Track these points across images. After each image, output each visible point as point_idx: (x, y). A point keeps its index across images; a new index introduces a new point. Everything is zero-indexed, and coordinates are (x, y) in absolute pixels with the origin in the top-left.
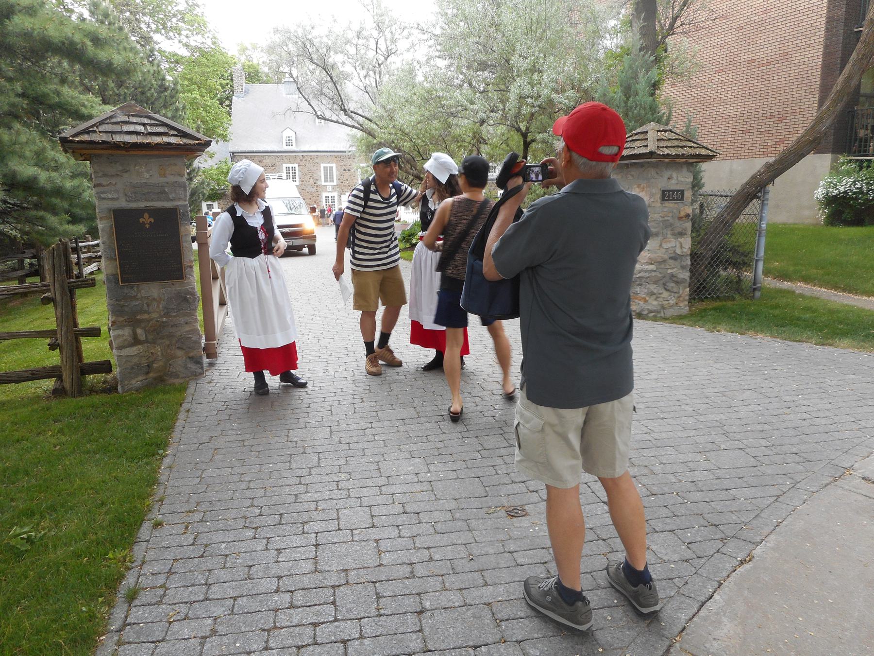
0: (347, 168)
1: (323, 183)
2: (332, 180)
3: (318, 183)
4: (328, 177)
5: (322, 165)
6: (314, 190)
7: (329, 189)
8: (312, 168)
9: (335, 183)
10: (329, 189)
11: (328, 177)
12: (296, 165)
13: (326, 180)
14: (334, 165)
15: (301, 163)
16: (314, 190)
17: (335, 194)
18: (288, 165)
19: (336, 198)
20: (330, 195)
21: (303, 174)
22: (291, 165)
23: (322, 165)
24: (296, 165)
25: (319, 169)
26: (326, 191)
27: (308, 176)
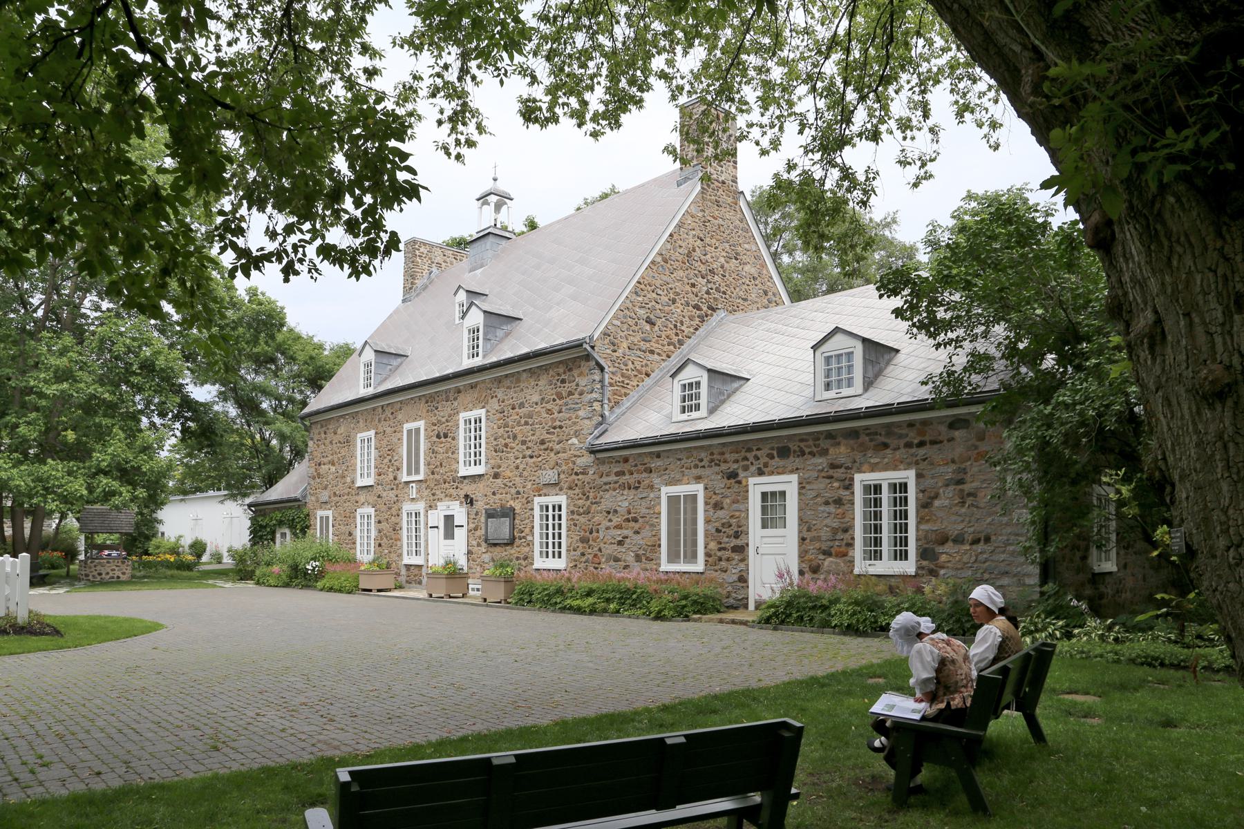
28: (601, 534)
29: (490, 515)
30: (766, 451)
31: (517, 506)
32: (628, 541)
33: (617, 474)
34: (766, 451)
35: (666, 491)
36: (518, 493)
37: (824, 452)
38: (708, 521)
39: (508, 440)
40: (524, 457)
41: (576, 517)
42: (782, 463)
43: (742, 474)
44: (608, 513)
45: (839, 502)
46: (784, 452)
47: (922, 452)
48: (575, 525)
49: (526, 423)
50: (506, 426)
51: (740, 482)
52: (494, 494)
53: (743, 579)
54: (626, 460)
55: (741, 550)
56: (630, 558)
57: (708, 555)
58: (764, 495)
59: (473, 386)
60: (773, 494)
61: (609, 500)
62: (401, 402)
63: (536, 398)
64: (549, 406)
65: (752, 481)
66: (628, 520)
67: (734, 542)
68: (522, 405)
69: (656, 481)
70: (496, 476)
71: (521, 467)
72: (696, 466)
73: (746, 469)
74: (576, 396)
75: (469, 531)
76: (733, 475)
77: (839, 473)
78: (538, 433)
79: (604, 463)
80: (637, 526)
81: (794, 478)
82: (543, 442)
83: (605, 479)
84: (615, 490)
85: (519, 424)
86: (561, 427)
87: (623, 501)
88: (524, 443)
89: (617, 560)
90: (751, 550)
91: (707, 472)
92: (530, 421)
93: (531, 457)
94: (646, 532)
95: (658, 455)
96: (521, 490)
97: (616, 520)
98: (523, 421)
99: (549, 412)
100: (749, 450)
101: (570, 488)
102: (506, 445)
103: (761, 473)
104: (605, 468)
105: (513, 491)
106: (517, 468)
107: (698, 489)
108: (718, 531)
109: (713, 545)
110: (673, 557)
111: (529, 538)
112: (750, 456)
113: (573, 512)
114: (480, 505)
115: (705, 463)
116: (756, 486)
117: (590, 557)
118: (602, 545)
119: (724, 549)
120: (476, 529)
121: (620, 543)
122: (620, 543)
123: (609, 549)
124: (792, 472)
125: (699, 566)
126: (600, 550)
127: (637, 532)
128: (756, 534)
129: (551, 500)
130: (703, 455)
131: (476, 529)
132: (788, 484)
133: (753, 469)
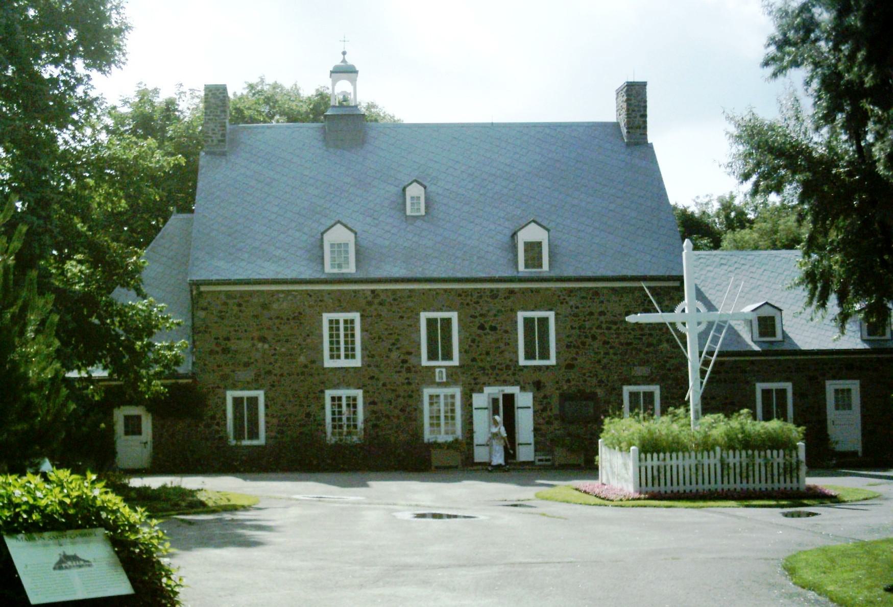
1: (425, 362)
2: (448, 356)
3: (412, 360)
6: (400, 379)
7: (441, 375)
9: (455, 362)
10: (441, 375)
12: (356, 316)
13: (432, 356)
14: (454, 316)
16: (400, 379)
17: (457, 391)
22: (341, 316)
23: (424, 316)
24: (356, 316)
26: (433, 383)
27: (387, 344)
31: (600, 392)
36: (601, 381)
38: (795, 405)
60: (843, 391)
68: (602, 313)
70: (570, 367)
75: (535, 412)
81: (857, 382)
85: (599, 327)
88: (605, 343)
92: (614, 327)
102: (584, 344)
105: (594, 381)
107: (788, 386)
113: (667, 398)
116: (831, 386)
124: (855, 379)
128: (831, 412)
132: (854, 386)
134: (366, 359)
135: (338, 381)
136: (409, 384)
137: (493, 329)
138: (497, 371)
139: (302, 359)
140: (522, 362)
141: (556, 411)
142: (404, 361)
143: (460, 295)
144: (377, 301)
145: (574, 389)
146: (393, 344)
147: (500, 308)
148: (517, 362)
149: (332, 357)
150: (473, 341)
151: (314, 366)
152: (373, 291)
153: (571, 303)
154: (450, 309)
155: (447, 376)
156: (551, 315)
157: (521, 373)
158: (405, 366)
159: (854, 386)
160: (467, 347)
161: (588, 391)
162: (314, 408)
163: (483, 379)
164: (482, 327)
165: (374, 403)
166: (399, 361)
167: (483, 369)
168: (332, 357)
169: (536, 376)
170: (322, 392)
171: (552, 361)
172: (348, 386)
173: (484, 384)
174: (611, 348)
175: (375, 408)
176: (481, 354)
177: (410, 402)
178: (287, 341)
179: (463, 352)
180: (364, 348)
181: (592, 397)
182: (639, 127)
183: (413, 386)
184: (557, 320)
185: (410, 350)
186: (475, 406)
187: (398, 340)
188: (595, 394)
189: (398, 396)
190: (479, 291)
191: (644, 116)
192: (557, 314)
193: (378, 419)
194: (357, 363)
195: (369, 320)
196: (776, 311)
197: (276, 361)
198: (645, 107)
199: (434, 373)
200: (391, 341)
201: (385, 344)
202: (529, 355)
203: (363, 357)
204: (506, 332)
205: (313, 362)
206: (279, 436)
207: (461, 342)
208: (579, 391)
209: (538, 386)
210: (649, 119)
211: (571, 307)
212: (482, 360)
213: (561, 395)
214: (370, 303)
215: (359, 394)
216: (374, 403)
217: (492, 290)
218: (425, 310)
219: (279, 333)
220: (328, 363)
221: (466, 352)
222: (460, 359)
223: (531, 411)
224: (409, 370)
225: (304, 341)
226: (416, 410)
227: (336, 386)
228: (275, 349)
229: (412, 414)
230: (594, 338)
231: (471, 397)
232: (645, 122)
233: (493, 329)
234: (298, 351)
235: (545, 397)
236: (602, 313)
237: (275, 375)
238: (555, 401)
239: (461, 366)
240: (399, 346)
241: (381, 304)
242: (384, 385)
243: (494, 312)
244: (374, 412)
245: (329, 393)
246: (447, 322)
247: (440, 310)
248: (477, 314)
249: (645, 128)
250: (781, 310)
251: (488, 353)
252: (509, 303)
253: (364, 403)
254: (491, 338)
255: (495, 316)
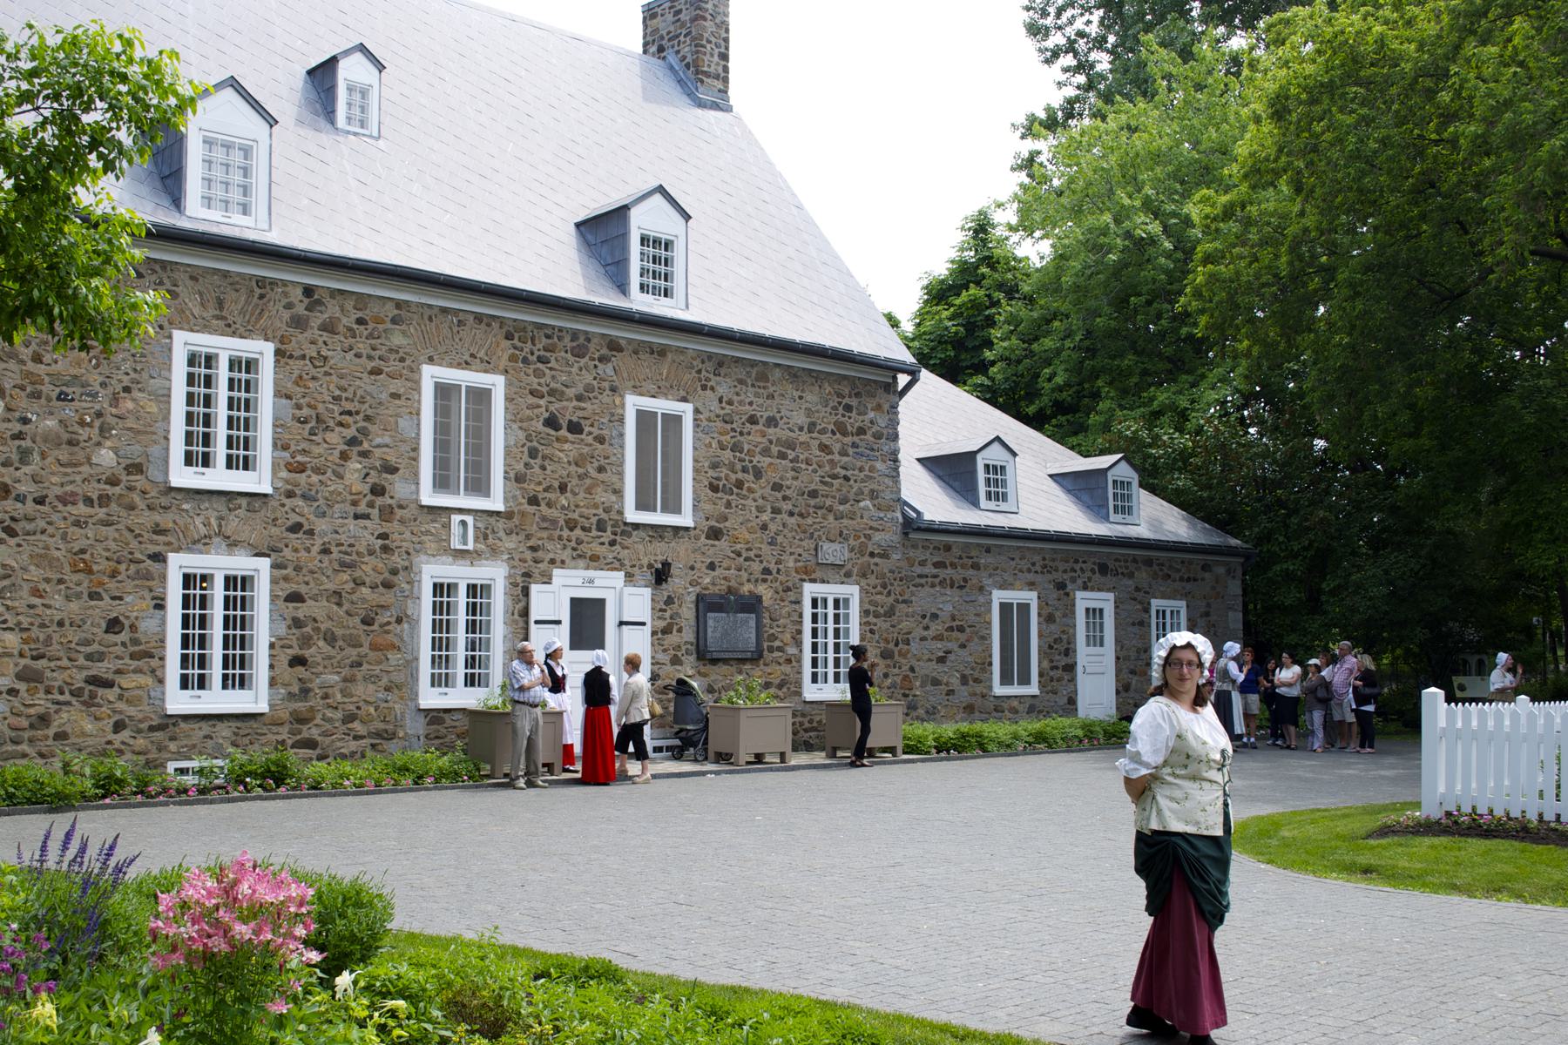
0: (568, 410)
1: (428, 497)
2: (479, 485)
3: (399, 488)
4: (462, 463)
5: (431, 375)
8: (366, 384)
9: (496, 502)
11: (462, 463)
12: (263, 350)
13: (443, 482)
15: (300, 342)
16: (364, 534)
17: (495, 574)
18: (206, 342)
19: (499, 602)
20: (461, 574)
21: (304, 423)
22: (226, 347)
23: (431, 375)
25: (407, 399)
28: (915, 647)
29: (706, 605)
30: (1089, 566)
32: (951, 657)
33: (936, 565)
34: (1089, 566)
35: (998, 596)
36: (767, 571)
37: (1131, 575)
38: (1040, 635)
39: (740, 475)
40: (776, 511)
41: (871, 619)
42: (1103, 579)
43: (1070, 587)
44: (924, 617)
45: (1141, 624)
46: (1103, 569)
47: (1189, 586)
48: (872, 631)
49: (782, 456)
50: (736, 448)
51: (1067, 594)
52: (712, 567)
53: (1072, 701)
54: (948, 548)
55: (1071, 668)
56: (955, 681)
57: (1041, 675)
58: (1087, 610)
59: (662, 352)
61: (924, 599)
62: (399, 304)
63: (800, 419)
64: (826, 439)
65: (1079, 595)
66: (951, 629)
67: (1064, 661)
68: (772, 422)
69: (986, 581)
70: (715, 534)
71: (773, 527)
72: (1029, 571)
73: (1073, 580)
74: (868, 437)
75: (654, 633)
76: (1061, 586)
77: (1140, 595)
78: (804, 477)
79: (914, 547)
80: (962, 637)
81: (1111, 596)
82: (813, 494)
83: (919, 570)
84: (933, 586)
85: (766, 452)
86: (847, 478)
87: (947, 602)
88: (777, 487)
89: (936, 682)
90: (1079, 669)
91: (1039, 578)
93: (791, 514)
94: (974, 646)
95: (988, 551)
96: (773, 567)
97: (936, 628)
98: (775, 449)
99: (824, 448)
100: (1076, 561)
101: (864, 576)
102: (739, 484)
103: (1085, 588)
104: (919, 554)
105: (756, 567)
106: (764, 527)
107: (1030, 597)
108: (1051, 647)
109: (1046, 664)
110: (1006, 679)
111: (792, 650)
112: (1077, 567)
114: (676, 583)
115: (1038, 568)
116: (1084, 600)
117: (898, 680)
118: (914, 662)
119: (1056, 668)
120: (666, 631)
121: (941, 660)
122: (941, 660)
123: (928, 668)
124: (1109, 590)
125: (1033, 689)
126: (912, 669)
127: (963, 646)
128: (1084, 654)
129: (831, 591)
130: (1037, 558)
131: (666, 631)
132: (1105, 601)
133: (1079, 582)
134: (284, 474)
135: (203, 530)
136: (385, 549)
137: (575, 428)
138: (578, 532)
139: (106, 457)
140: (632, 515)
141: (689, 635)
142: (378, 491)
143: (509, 337)
144: (317, 319)
145: (721, 587)
146: (352, 442)
147: (588, 378)
148: (620, 513)
149: (189, 460)
150: (533, 453)
151: (139, 481)
152: (308, 291)
153: (721, 390)
154: (488, 366)
155: (476, 539)
156: (686, 410)
157: (628, 541)
158: (379, 501)
159: (1105, 601)
160: (520, 467)
161: (746, 589)
162: (135, 604)
163: (554, 549)
164: (552, 422)
165: (295, 598)
166: (366, 489)
167: (554, 522)
168: (189, 460)
169: (659, 552)
170: (159, 558)
171: (685, 519)
172: (233, 544)
173: (552, 562)
174: (785, 498)
175: (302, 611)
176: (545, 490)
177: (387, 597)
178: (63, 397)
179: (516, 478)
180: (279, 445)
181: (752, 605)
182: (717, 77)
183: (397, 560)
184: (697, 423)
185: (392, 459)
186: (534, 616)
187: (364, 432)
188: (759, 599)
189: (359, 583)
190: (549, 332)
191: (725, 57)
192: (697, 411)
193: (306, 641)
194: (258, 481)
195: (296, 365)
196: (1008, 456)
197: (24, 456)
198: (726, 40)
199: (447, 526)
200: (350, 432)
201: (334, 437)
202: (643, 504)
203: (275, 467)
204: (601, 440)
205: (136, 468)
206: (22, 686)
207: (508, 453)
208: (730, 590)
209: (661, 575)
210: (730, 65)
211: (720, 400)
212: (549, 505)
213: (700, 599)
214: (299, 323)
215: (261, 568)
216: (295, 598)
217: (575, 335)
218: (431, 360)
219: (40, 369)
220: (182, 476)
221: (519, 479)
222: (506, 499)
223: (647, 629)
224: (387, 514)
225: (115, 401)
226: (399, 621)
227: (199, 543)
228: (25, 421)
229: (377, 631)
230: (758, 474)
231: (526, 592)
232: (726, 69)
233: (575, 428)
234: (95, 436)
235: (669, 601)
236: (772, 422)
237: (21, 499)
238: (688, 612)
239: (508, 515)
240: (366, 445)
241: (329, 327)
242: (326, 551)
243: (580, 389)
244: (297, 623)
245: (179, 563)
246: (481, 397)
247: (466, 365)
248: (545, 390)
249: (726, 80)
250: (1014, 454)
251: (563, 488)
252: (608, 369)
253: (274, 598)
254: (568, 449)
255: (579, 398)
